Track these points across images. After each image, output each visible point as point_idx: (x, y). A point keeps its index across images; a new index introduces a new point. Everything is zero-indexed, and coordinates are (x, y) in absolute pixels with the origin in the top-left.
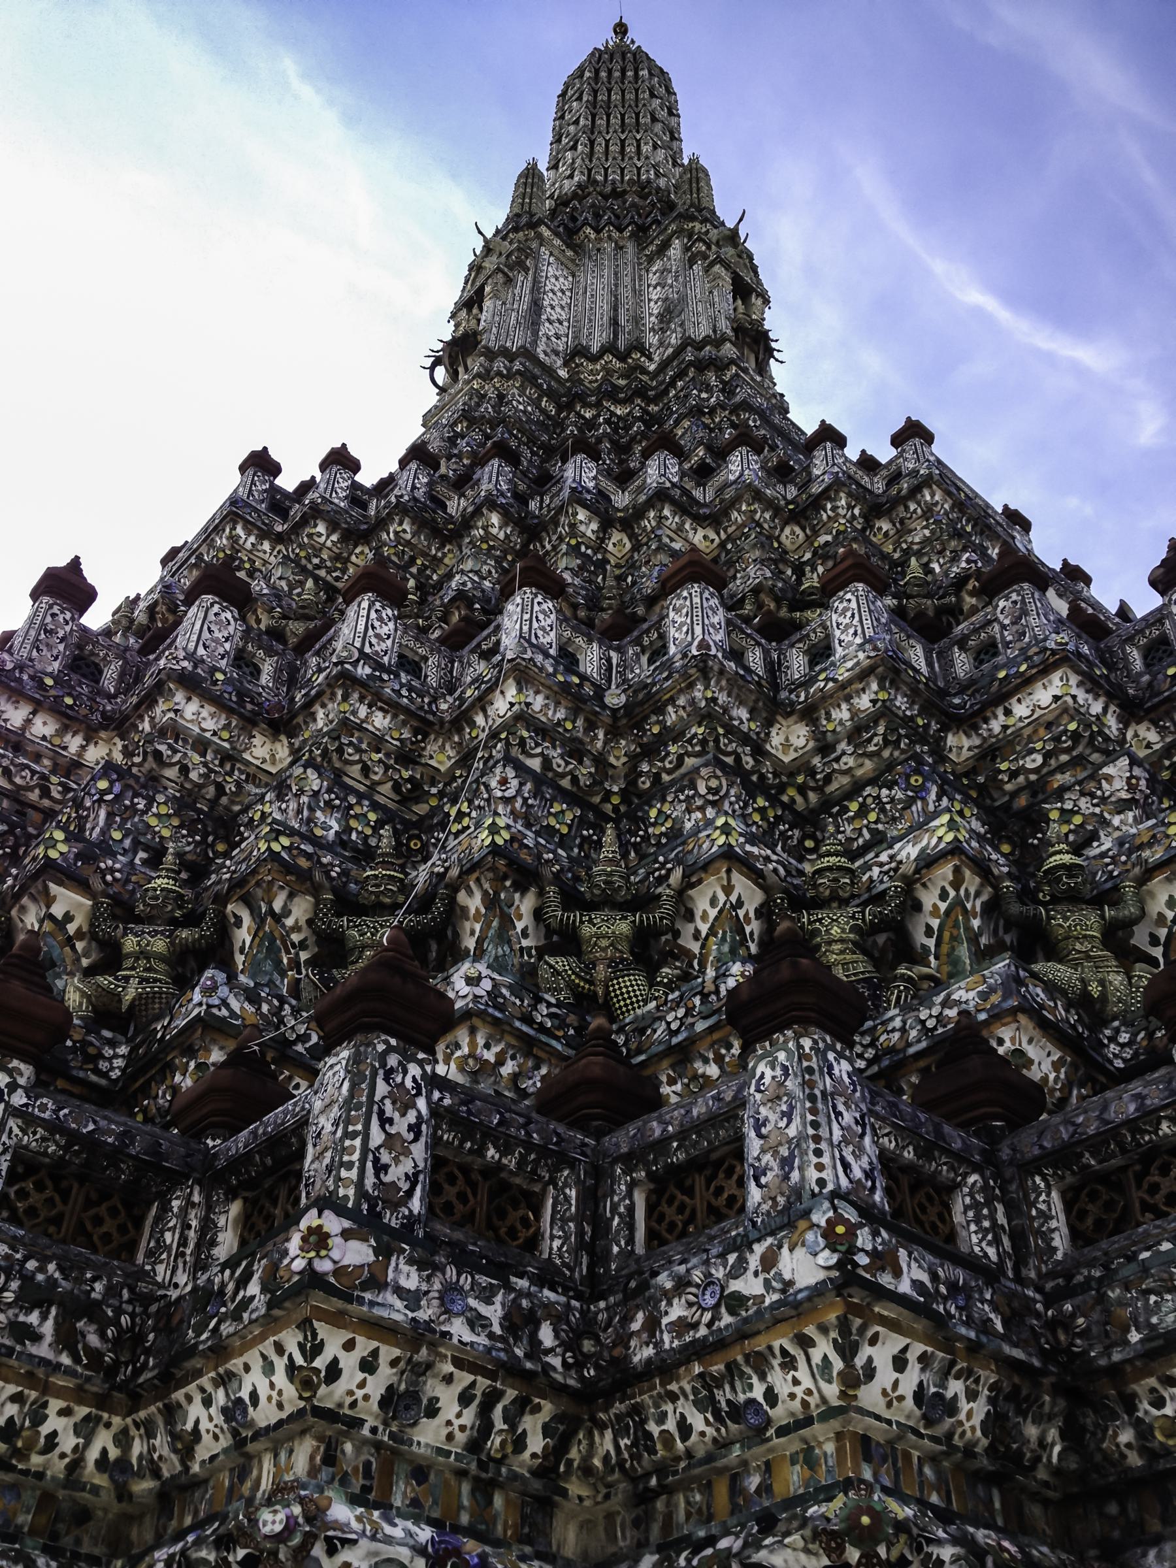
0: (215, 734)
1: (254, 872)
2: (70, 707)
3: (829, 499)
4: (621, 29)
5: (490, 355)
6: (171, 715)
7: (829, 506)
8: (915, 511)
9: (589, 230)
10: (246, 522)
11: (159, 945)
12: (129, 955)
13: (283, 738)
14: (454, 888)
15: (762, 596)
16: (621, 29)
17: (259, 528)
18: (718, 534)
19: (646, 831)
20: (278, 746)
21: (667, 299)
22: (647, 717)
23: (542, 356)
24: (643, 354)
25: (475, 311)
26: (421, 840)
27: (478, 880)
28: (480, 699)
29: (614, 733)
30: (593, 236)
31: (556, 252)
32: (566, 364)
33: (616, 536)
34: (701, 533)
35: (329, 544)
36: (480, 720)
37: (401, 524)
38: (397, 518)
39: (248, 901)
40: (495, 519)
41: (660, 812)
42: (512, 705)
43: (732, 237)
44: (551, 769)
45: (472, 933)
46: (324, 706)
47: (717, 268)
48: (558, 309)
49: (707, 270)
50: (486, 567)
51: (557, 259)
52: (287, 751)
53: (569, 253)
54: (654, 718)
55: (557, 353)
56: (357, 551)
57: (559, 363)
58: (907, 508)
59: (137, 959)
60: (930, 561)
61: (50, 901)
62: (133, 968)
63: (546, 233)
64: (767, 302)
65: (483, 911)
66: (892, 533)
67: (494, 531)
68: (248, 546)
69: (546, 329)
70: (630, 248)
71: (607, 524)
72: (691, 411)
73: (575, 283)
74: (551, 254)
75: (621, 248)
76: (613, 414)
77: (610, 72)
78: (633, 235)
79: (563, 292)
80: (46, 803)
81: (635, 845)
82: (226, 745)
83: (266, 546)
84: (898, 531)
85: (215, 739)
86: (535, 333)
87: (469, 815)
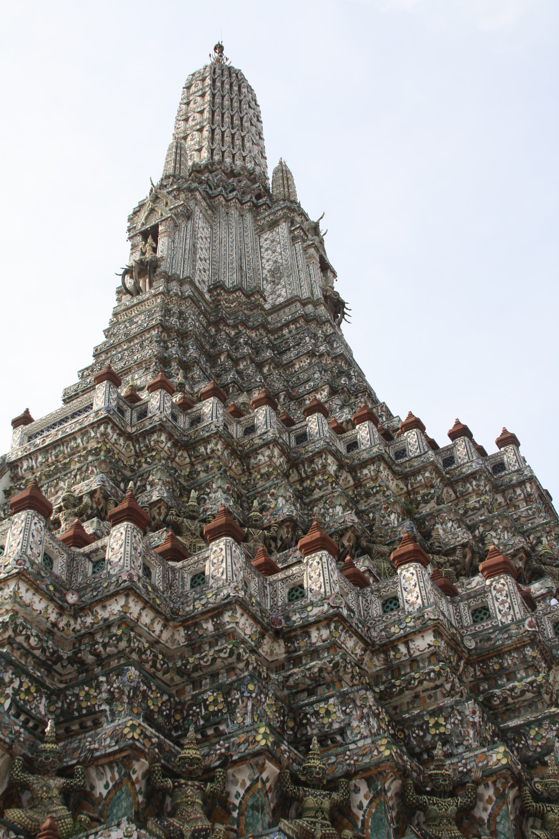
0: (250, 637)
1: (377, 765)
2: (158, 605)
3: (475, 478)
4: (219, 48)
5: (169, 279)
6: (234, 625)
7: (474, 483)
8: (520, 495)
9: (222, 199)
10: (114, 424)
11: (327, 804)
12: (310, 809)
13: (282, 642)
14: (477, 783)
15: (467, 550)
16: (219, 48)
17: (120, 430)
18: (407, 486)
19: (526, 742)
20: (276, 646)
21: (276, 262)
22: (492, 658)
23: (197, 284)
24: (262, 296)
25: (150, 240)
26: (404, 733)
27: (494, 783)
28: (405, 636)
29: (468, 663)
30: (224, 203)
31: (203, 211)
32: (210, 291)
33: (345, 474)
34: (395, 482)
35: (166, 449)
36: (403, 649)
37: (216, 444)
38: (214, 441)
39: (370, 782)
40: (276, 452)
41: (537, 733)
42: (430, 646)
43: (315, 228)
44: (454, 690)
45: (485, 809)
46: (318, 629)
47: (312, 251)
48: (204, 251)
49: (305, 250)
50: (288, 494)
51: (204, 215)
52: (283, 650)
53: (210, 212)
54: (495, 660)
55: (204, 282)
56: (179, 454)
57: (206, 289)
58: (515, 492)
59: (317, 812)
60: (542, 536)
61: (262, 768)
62: (315, 817)
63: (199, 197)
64: (335, 276)
65: (494, 798)
66: (503, 504)
67: (275, 460)
68: (113, 441)
69: (200, 265)
70: (249, 217)
71: (341, 467)
72: (308, 352)
73: (212, 233)
74: (201, 211)
75: (242, 216)
76: (249, 338)
77: (223, 83)
78: (250, 210)
79: (206, 238)
80: (153, 670)
81: (518, 749)
82: (253, 643)
83: (122, 441)
84: (507, 504)
85: (249, 640)
86: (194, 268)
87: (445, 726)
